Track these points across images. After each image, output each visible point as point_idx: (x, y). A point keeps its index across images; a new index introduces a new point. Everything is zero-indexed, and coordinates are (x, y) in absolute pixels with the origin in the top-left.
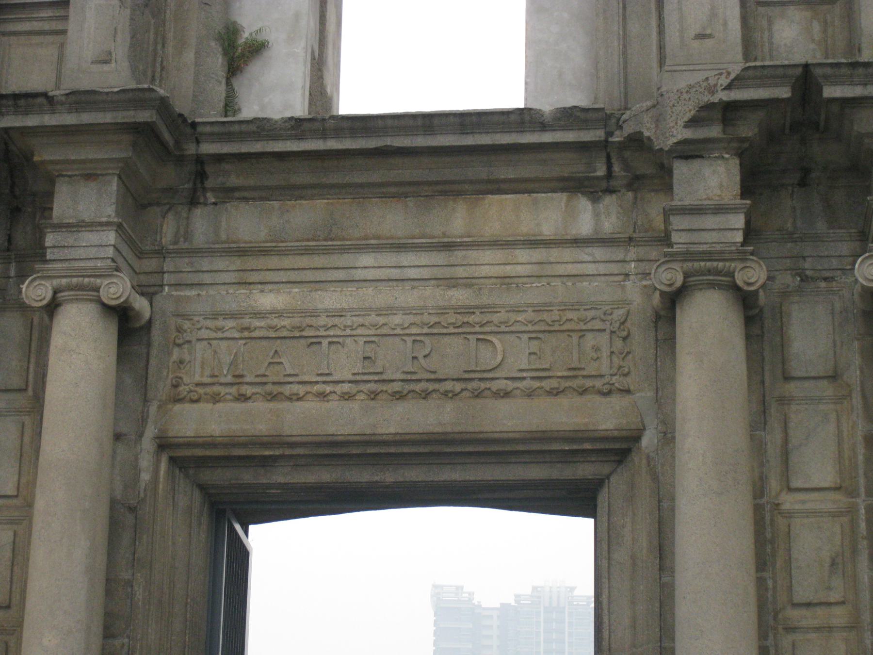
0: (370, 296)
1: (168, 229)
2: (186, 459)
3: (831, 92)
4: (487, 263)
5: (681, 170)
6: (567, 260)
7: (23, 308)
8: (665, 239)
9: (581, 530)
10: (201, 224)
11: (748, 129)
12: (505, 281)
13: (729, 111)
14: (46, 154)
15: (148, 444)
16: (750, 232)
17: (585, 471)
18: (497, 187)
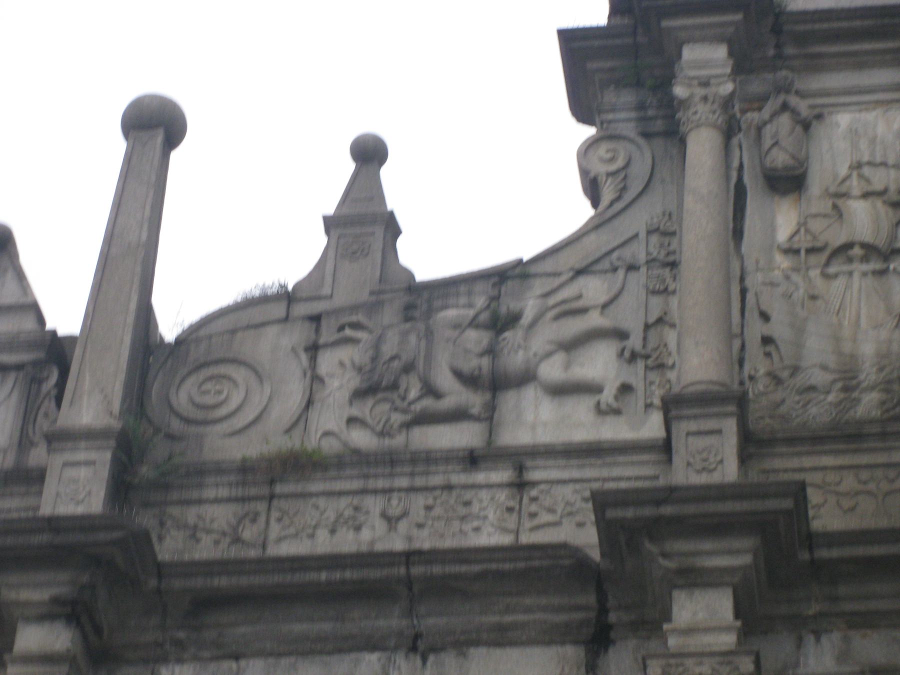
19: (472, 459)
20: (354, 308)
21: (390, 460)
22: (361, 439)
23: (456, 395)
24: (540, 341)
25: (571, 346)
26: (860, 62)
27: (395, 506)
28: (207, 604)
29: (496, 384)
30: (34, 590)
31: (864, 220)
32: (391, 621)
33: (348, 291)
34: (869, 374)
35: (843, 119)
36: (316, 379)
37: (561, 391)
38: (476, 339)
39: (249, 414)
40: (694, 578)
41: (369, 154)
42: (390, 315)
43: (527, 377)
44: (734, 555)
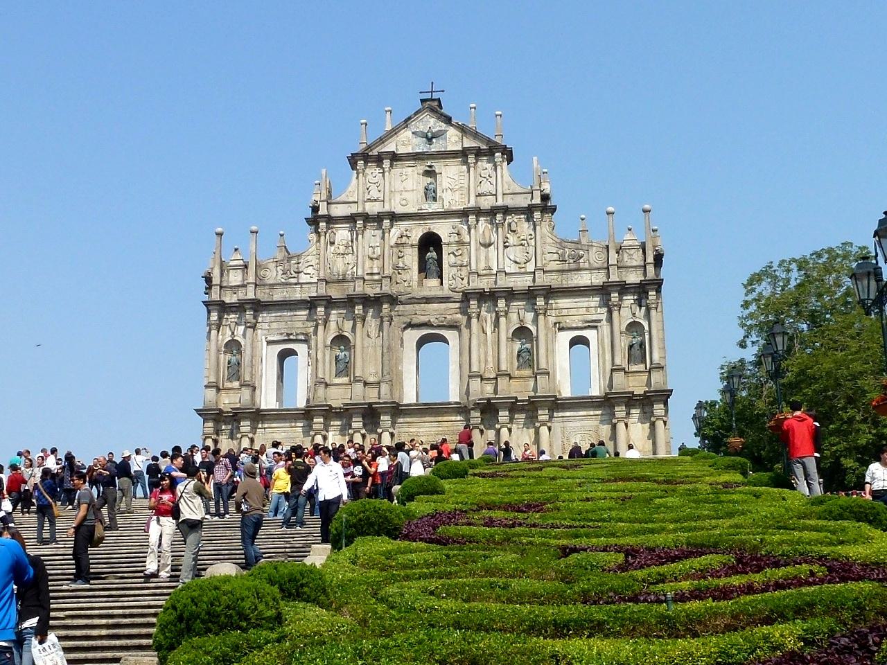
0: (427, 429)
5: (472, 412)
18: (446, 412)
19: (296, 284)
20: (281, 260)
21: (287, 284)
22: (283, 280)
23: (295, 275)
26: (342, 223)
27: (287, 290)
29: (298, 273)
30: (247, 306)
31: (342, 249)
32: (288, 307)
34: (341, 274)
35: (340, 231)
36: (277, 272)
37: (305, 274)
39: (270, 276)
42: (286, 262)
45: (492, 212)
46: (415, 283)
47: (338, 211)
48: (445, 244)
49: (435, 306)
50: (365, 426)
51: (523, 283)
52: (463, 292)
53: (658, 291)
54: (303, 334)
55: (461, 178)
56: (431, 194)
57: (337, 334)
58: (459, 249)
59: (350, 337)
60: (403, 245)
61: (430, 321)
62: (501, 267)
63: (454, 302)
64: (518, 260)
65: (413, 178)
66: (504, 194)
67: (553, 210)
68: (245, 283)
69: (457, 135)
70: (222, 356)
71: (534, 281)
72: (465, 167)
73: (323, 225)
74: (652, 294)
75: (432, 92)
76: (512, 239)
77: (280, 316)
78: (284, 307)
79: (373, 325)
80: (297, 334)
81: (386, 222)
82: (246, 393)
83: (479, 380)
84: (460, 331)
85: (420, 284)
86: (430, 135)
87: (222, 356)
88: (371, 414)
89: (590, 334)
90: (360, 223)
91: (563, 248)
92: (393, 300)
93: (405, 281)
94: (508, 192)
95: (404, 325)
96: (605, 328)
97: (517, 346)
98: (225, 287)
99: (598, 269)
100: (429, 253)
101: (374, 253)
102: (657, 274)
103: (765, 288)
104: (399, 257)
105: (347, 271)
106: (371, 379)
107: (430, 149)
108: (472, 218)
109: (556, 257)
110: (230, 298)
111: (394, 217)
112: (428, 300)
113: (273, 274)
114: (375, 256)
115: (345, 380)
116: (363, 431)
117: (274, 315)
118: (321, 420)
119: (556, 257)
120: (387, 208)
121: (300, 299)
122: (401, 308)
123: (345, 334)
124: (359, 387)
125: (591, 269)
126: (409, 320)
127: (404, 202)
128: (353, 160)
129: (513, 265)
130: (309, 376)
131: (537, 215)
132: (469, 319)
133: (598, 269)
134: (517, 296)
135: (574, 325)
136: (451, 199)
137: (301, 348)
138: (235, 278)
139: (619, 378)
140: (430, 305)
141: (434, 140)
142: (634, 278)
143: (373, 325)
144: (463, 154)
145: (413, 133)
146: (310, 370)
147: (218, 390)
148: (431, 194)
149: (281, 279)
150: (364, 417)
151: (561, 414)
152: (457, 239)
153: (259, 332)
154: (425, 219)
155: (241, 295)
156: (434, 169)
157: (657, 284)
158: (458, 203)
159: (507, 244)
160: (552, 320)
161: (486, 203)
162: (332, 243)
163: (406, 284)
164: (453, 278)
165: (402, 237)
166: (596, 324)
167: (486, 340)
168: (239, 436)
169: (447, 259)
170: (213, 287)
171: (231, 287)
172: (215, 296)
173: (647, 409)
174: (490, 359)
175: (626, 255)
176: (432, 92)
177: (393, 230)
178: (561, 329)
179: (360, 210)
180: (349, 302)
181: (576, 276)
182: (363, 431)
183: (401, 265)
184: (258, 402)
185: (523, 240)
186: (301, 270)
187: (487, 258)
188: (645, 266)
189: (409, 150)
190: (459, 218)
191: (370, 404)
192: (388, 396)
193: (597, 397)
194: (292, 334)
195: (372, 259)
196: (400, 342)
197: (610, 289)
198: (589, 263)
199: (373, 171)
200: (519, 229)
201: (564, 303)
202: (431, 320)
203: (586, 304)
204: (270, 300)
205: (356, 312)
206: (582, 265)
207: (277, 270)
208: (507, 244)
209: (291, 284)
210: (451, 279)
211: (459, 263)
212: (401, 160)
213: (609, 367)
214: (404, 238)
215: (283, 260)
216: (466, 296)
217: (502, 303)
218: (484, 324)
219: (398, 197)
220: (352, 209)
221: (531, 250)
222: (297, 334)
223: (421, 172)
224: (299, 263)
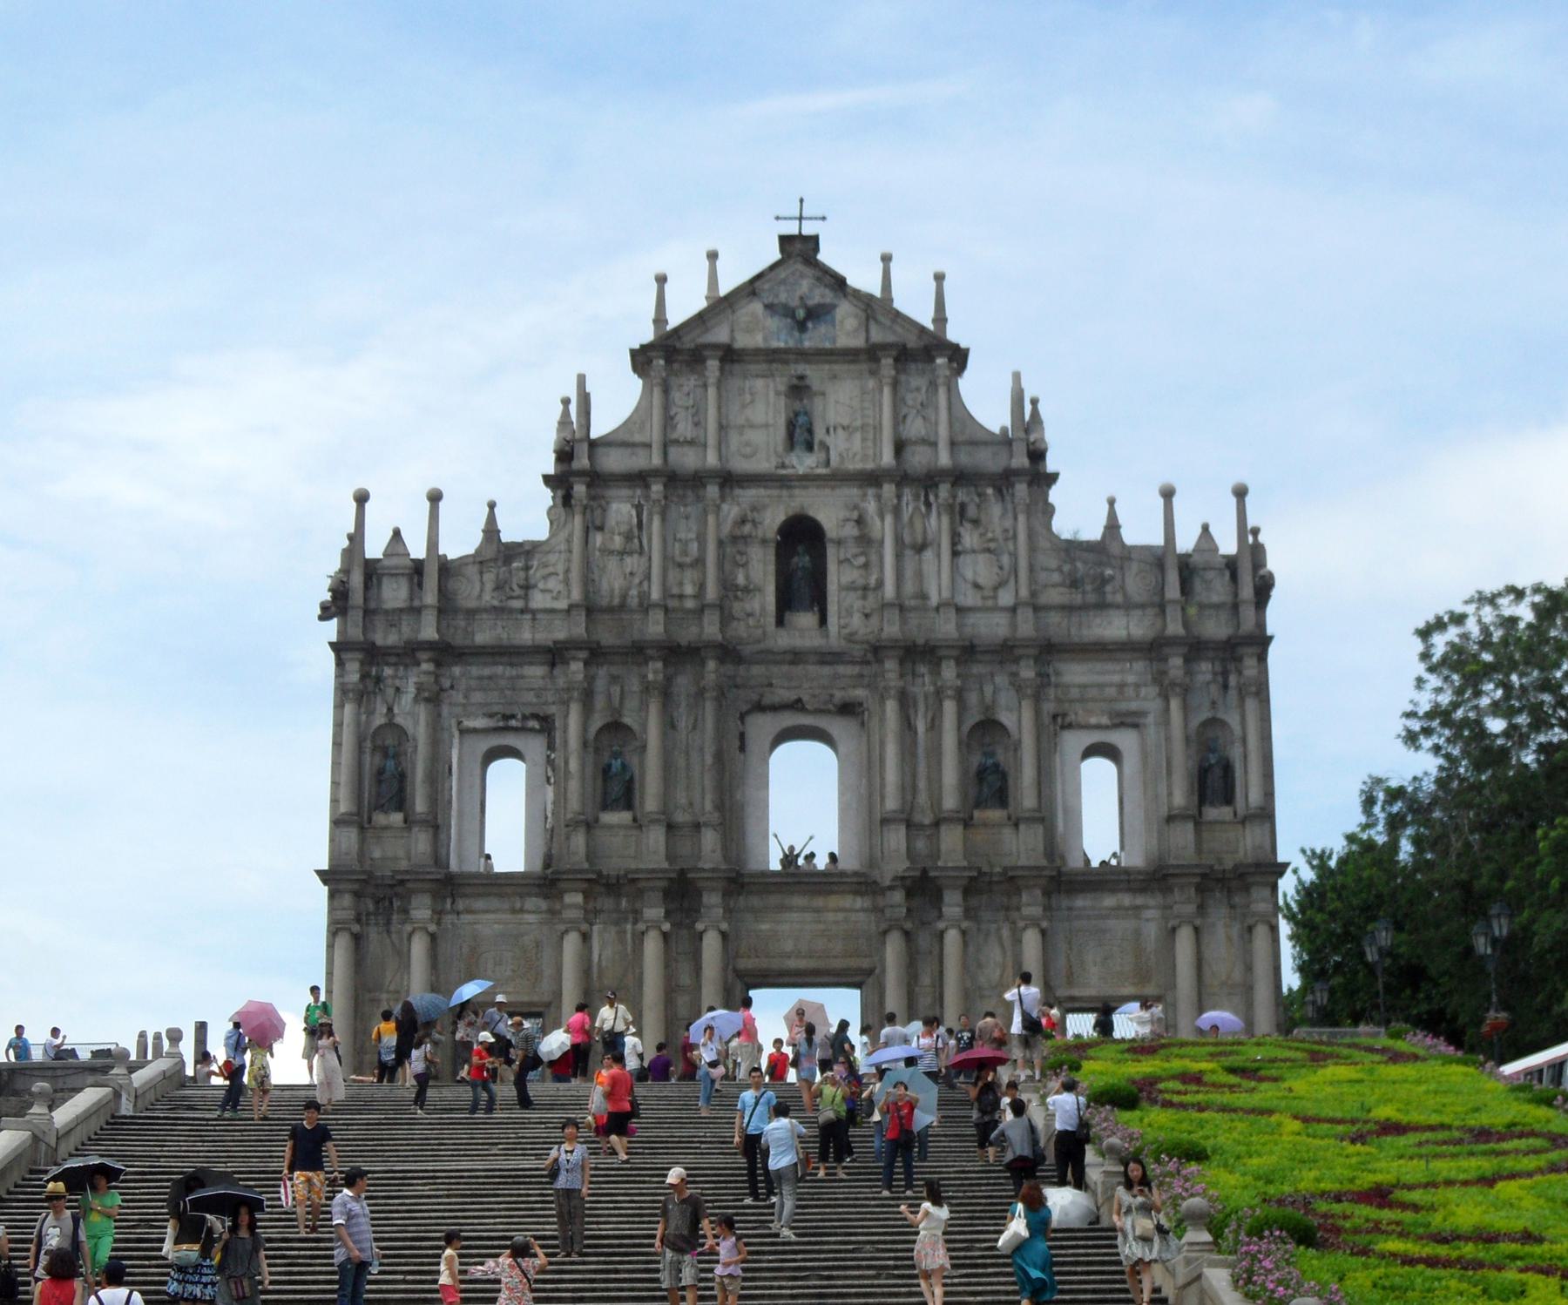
1: (732, 904)
2: (739, 974)
3: (932, 874)
4: (831, 916)
6: (853, 916)
7: (691, 926)
8: (882, 911)
9: (856, 993)
10: (741, 901)
11: (908, 882)
12: (836, 922)
13: (903, 878)
14: (700, 884)
15: (730, 972)
16: (909, 910)
17: (857, 979)
18: (831, 893)
19: (522, 611)
22: (496, 603)
23: (518, 592)
24: (538, 575)
25: (545, 578)
28: (462, 655)
29: (527, 587)
30: (423, 656)
32: (505, 659)
33: (490, 553)
34: (617, 592)
35: (614, 506)
36: (482, 583)
37: (543, 591)
38: (522, 574)
40: (574, 658)
41: (492, 506)
43: (535, 586)
44: (583, 654)
45: (928, 481)
46: (772, 620)
47: (614, 462)
48: (832, 541)
49: (811, 668)
50: (668, 915)
51: (991, 627)
52: (867, 642)
53: (1262, 658)
54: (535, 716)
55: (866, 405)
56: (800, 433)
57: (609, 719)
58: (862, 554)
59: (635, 727)
60: (745, 539)
61: (799, 700)
62: (946, 594)
63: (853, 663)
64: (981, 581)
65: (768, 403)
66: (953, 444)
67: (1053, 478)
68: (416, 603)
69: (856, 316)
70: (367, 758)
71: (1013, 626)
72: (871, 384)
73: (580, 489)
74: (1250, 663)
75: (801, 218)
76: (969, 538)
77: (490, 678)
78: (498, 659)
79: (684, 704)
80: (525, 718)
81: (712, 491)
82: (421, 842)
83: (903, 829)
84: (863, 724)
85: (780, 622)
86: (801, 314)
87: (367, 758)
88: (681, 892)
89: (1125, 740)
90: (657, 488)
91: (1072, 561)
92: (728, 652)
93: (749, 615)
94: (960, 438)
95: (745, 708)
96: (1152, 731)
97: (976, 760)
98: (374, 612)
99: (1142, 606)
100: (796, 559)
101: (685, 553)
102: (1261, 624)
103: (1440, 643)
104: (738, 565)
105: (629, 589)
106: (680, 817)
107: (801, 341)
108: (889, 489)
109: (1056, 577)
110: (385, 637)
111: (729, 480)
112: (796, 657)
113: (475, 591)
114: (688, 560)
115: (624, 817)
116: (666, 927)
117: (475, 671)
118: (578, 898)
119: (1056, 577)
120: (712, 460)
121: (530, 643)
122: (742, 670)
123: (627, 720)
124: (656, 838)
125: (1128, 606)
126: (755, 697)
127: (748, 450)
128: (641, 359)
129: (970, 592)
130: (550, 807)
131: (1021, 489)
132: (882, 699)
133: (1142, 606)
134: (979, 657)
135: (1093, 721)
136: (847, 450)
137: (534, 746)
138: (394, 594)
139: (1184, 835)
140: (798, 670)
141: (810, 325)
142: (1215, 628)
143: (684, 704)
144: (871, 353)
145: (769, 307)
146: (550, 792)
147: (362, 828)
148: (800, 433)
149: (489, 599)
150: (667, 894)
151: (1065, 903)
152: (855, 532)
153: (445, 710)
154: (789, 487)
155: (406, 631)
156: (808, 382)
157: (1261, 642)
158: (858, 457)
159: (959, 548)
160: (1049, 707)
161: (918, 459)
162: (601, 528)
163: (751, 622)
164: (847, 614)
165: (743, 521)
166: (1136, 720)
167: (915, 743)
168: (409, 928)
169: (837, 576)
170: (351, 613)
171: (387, 612)
172: (356, 633)
173: (1237, 899)
174: (922, 784)
175: (1198, 585)
176: (801, 218)
177: (725, 507)
178: (1069, 726)
179: (657, 461)
180: (637, 652)
181: (1098, 621)
182: (666, 927)
183: (741, 580)
184: (443, 851)
185: (991, 540)
186: (532, 582)
187: (919, 575)
188: (1235, 607)
189: (756, 340)
190: (860, 487)
191: (682, 872)
192: (718, 855)
193: (1139, 872)
194: (513, 717)
195: (681, 566)
196: (737, 743)
197: (1166, 650)
198: (1125, 595)
199: (682, 380)
200: (983, 517)
201: (1075, 674)
202: (805, 698)
203: (1116, 678)
204: (468, 642)
205: (651, 677)
206: (1109, 598)
207: (482, 583)
208: (959, 548)
209: (511, 611)
210: (844, 613)
211: (861, 582)
212: (738, 361)
213: (1164, 811)
214: (747, 528)
215: (495, 560)
216: (878, 650)
217: (949, 672)
218: (911, 712)
219: (734, 440)
220: (638, 462)
221: (1005, 560)
222: (525, 718)
223: (782, 388)
224: (527, 568)
